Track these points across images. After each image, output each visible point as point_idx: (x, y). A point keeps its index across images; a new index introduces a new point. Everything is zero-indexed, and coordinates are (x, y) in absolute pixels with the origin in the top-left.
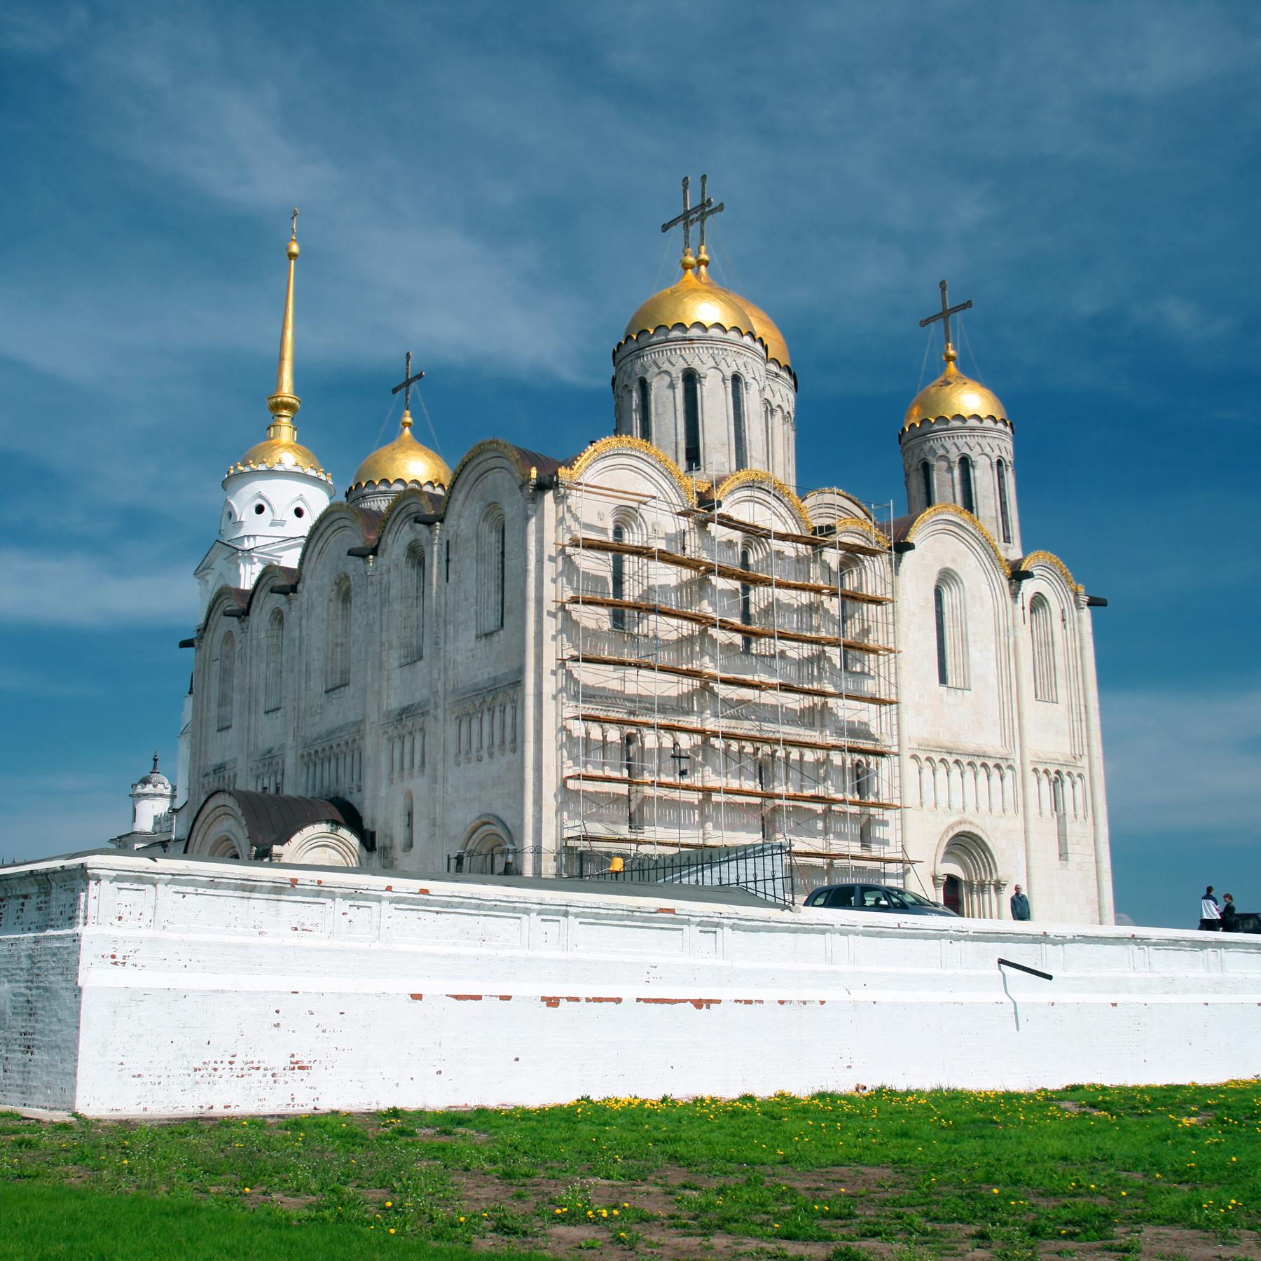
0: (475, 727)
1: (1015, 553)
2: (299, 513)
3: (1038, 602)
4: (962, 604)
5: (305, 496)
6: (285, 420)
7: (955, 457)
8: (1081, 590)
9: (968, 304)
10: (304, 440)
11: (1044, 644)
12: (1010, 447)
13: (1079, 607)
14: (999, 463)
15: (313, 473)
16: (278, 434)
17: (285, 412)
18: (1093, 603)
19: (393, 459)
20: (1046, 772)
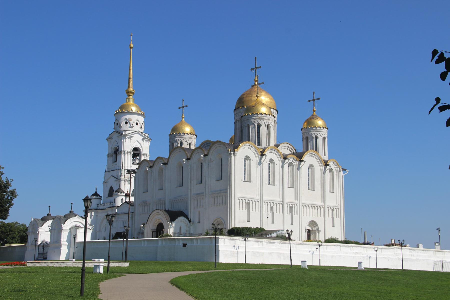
0: (216, 199)
1: (326, 158)
2: (137, 124)
3: (331, 170)
4: (314, 172)
5: (139, 119)
6: (131, 97)
7: (314, 136)
8: (341, 167)
9: (319, 99)
10: (136, 102)
11: (331, 180)
12: (327, 134)
13: (340, 171)
14: (324, 137)
15: (140, 113)
16: (129, 101)
17: (131, 94)
18: (344, 170)
19: (181, 128)
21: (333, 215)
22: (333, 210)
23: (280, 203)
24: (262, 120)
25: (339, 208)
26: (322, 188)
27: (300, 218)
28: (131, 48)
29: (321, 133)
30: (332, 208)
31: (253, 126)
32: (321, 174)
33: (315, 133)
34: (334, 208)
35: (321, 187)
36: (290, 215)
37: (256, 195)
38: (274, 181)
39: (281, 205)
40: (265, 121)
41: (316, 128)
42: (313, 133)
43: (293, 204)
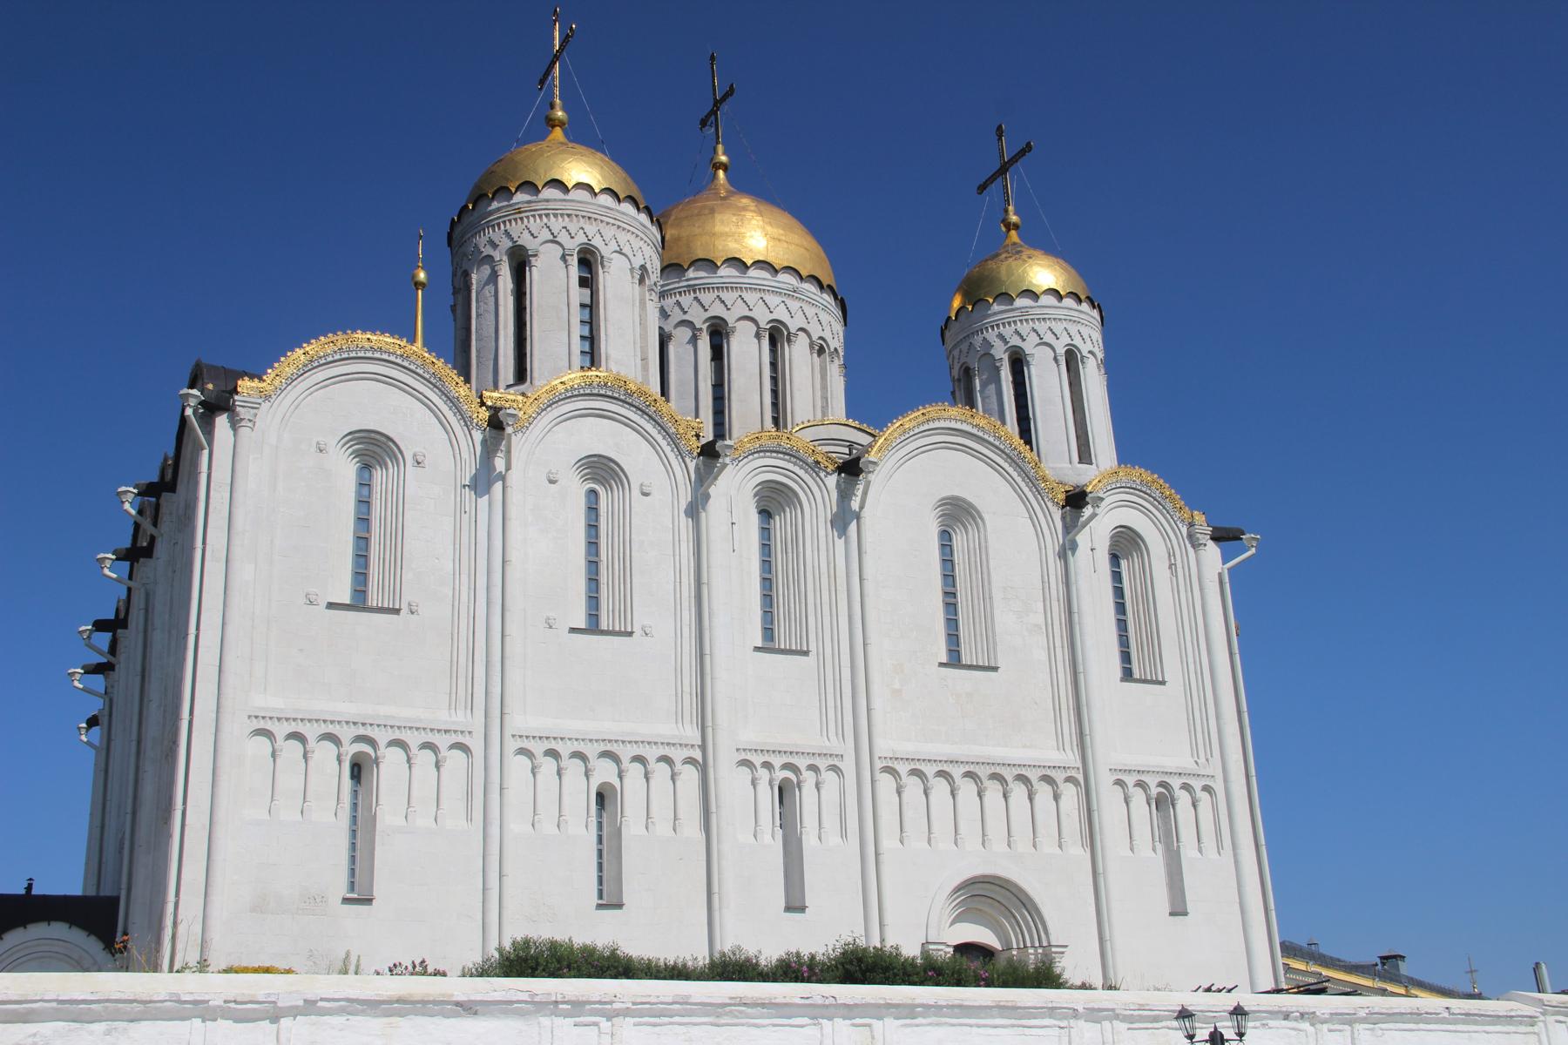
4: (983, 548)
7: (1000, 353)
13: (1196, 545)
18: (1219, 537)
20: (1140, 784)
21: (1168, 838)
22: (1163, 802)
23: (678, 755)
24: (534, 224)
25: (1218, 786)
26: (1062, 654)
27: (871, 860)
28: (418, 284)
29: (1042, 327)
30: (1152, 781)
31: (486, 270)
32: (1044, 563)
33: (1007, 331)
34: (1176, 783)
35: (1051, 650)
36: (773, 843)
37: (452, 706)
38: (626, 608)
39: (690, 776)
40: (556, 224)
41: (1011, 300)
42: (991, 336)
43: (802, 763)
